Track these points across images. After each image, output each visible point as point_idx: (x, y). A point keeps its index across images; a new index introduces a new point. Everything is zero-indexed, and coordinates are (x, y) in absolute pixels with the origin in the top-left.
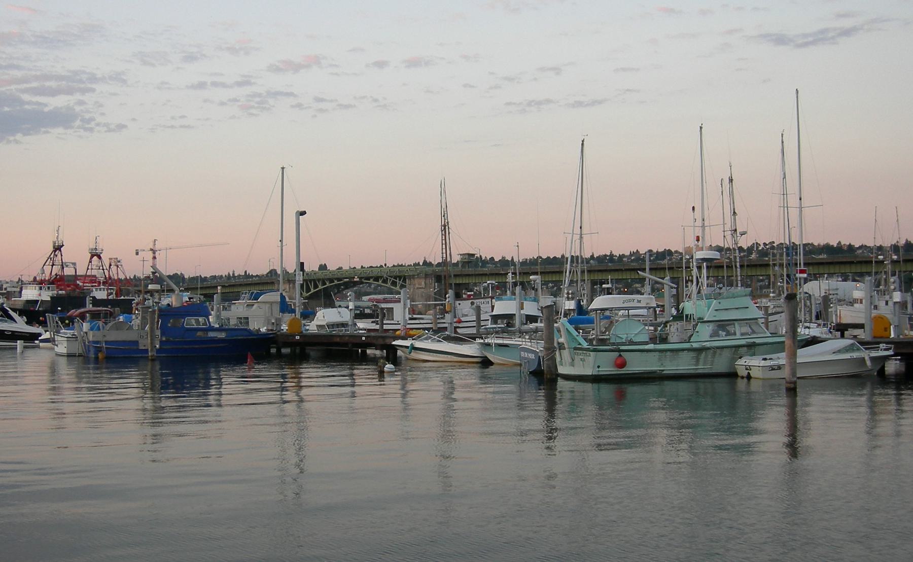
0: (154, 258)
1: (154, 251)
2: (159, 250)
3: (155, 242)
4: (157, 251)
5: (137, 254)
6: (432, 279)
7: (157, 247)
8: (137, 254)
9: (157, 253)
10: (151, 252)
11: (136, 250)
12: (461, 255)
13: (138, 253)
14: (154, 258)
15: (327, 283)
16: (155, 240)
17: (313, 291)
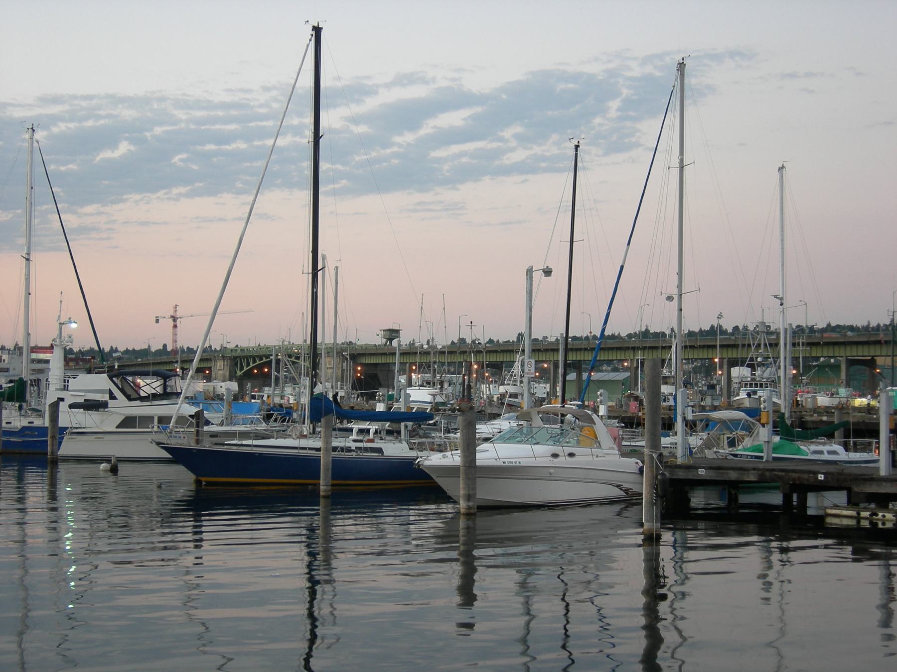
0: (175, 326)
1: (174, 319)
2: (180, 318)
3: (176, 308)
4: (178, 318)
5: (157, 321)
6: (340, 359)
7: (178, 314)
8: (157, 321)
9: (178, 321)
10: (171, 319)
11: (156, 317)
12: (384, 331)
13: (158, 320)
14: (175, 326)
15: (258, 361)
16: (176, 305)
17: (245, 369)
